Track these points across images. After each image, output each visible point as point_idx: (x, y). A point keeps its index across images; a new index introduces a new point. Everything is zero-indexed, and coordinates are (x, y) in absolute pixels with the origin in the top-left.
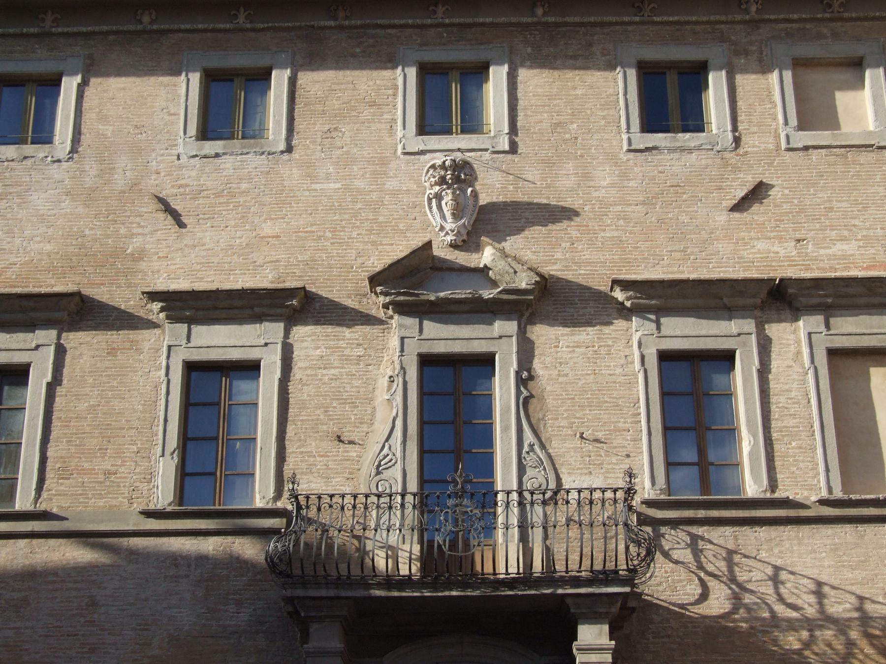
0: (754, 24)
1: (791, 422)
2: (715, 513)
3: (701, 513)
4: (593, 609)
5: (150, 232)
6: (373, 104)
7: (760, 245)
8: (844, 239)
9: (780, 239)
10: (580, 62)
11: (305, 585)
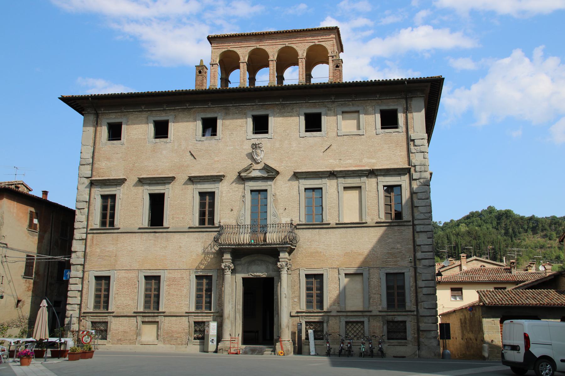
0: (333, 102)
1: (333, 205)
2: (314, 226)
3: (311, 227)
4: (284, 250)
6: (240, 126)
7: (331, 161)
8: (350, 159)
9: (335, 159)
10: (290, 114)
11: (223, 245)
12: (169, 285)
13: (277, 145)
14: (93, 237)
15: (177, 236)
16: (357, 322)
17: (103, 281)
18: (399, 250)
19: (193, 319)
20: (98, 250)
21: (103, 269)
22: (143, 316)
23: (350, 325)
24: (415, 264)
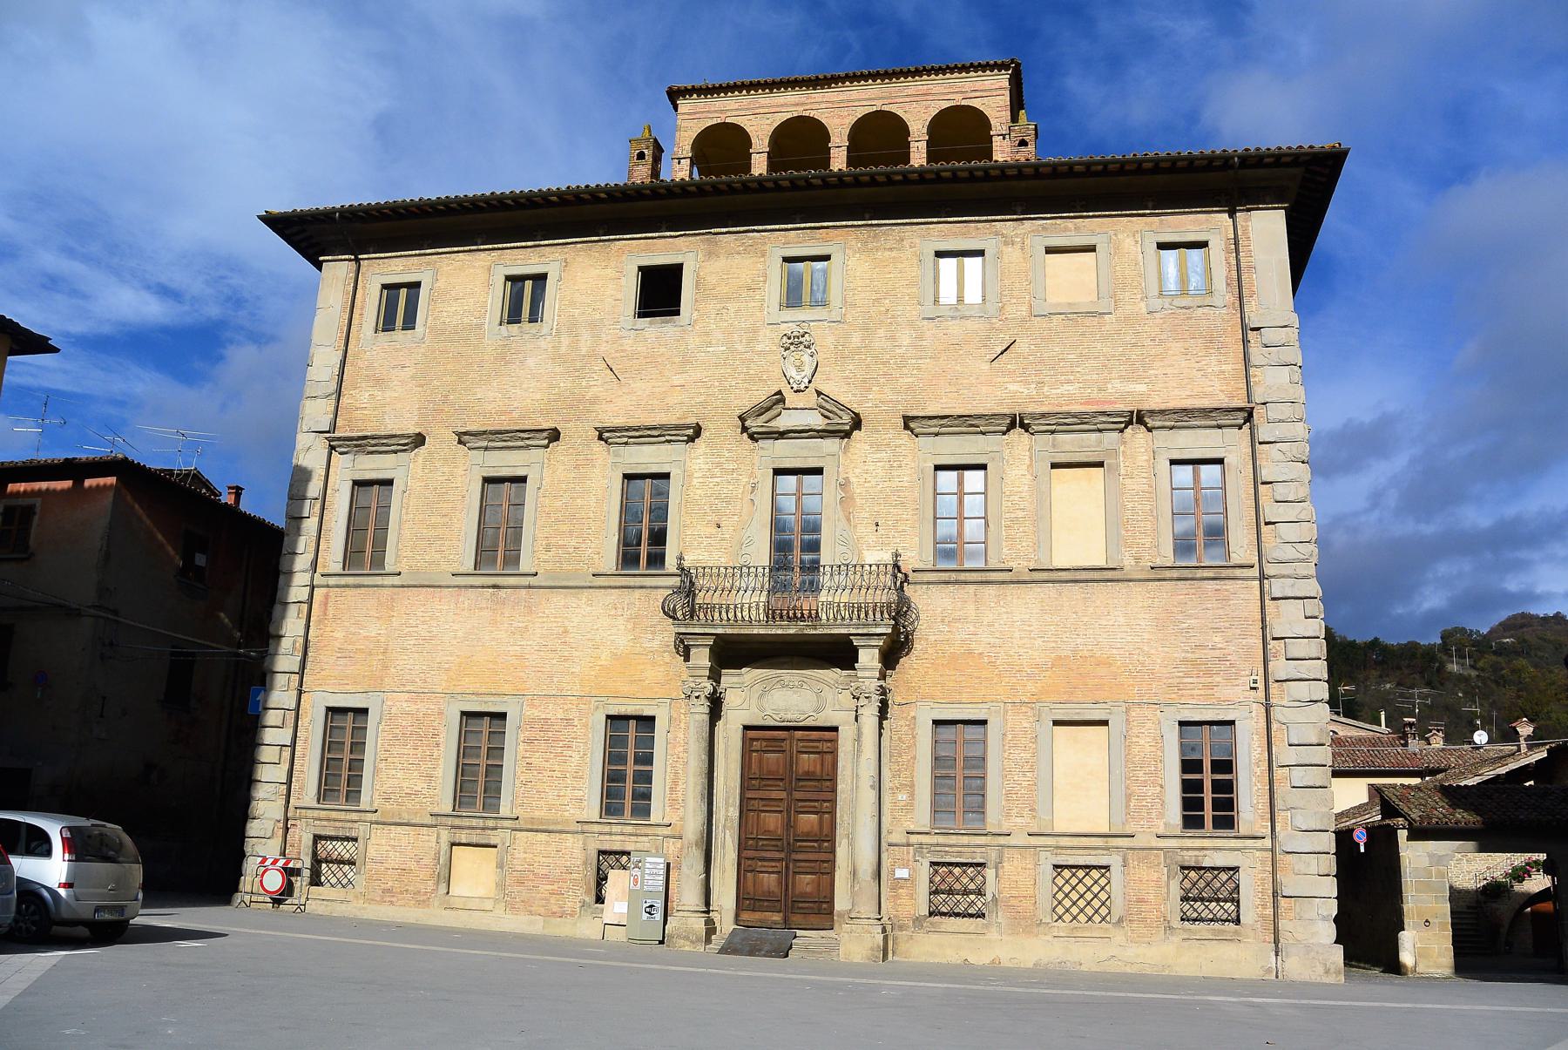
1: (1020, 514)
5: (597, 383)
7: (1012, 387)
9: (1027, 383)
12: (529, 741)
13: (856, 339)
14: (327, 597)
15: (558, 598)
16: (1088, 868)
17: (346, 721)
18: (1217, 653)
19: (595, 844)
20: (339, 634)
21: (349, 688)
22: (453, 827)
23: (1067, 873)
24: (1267, 697)
